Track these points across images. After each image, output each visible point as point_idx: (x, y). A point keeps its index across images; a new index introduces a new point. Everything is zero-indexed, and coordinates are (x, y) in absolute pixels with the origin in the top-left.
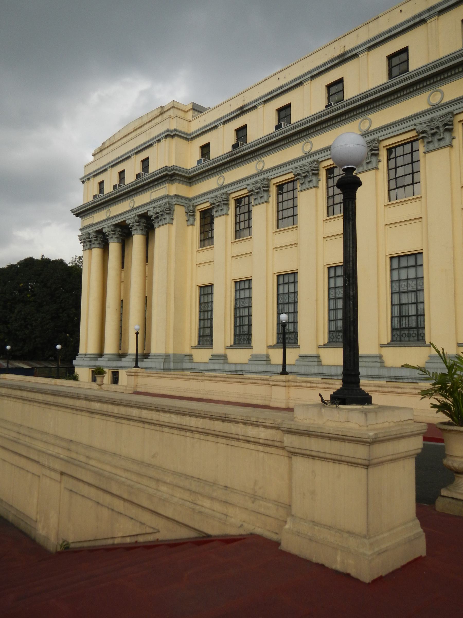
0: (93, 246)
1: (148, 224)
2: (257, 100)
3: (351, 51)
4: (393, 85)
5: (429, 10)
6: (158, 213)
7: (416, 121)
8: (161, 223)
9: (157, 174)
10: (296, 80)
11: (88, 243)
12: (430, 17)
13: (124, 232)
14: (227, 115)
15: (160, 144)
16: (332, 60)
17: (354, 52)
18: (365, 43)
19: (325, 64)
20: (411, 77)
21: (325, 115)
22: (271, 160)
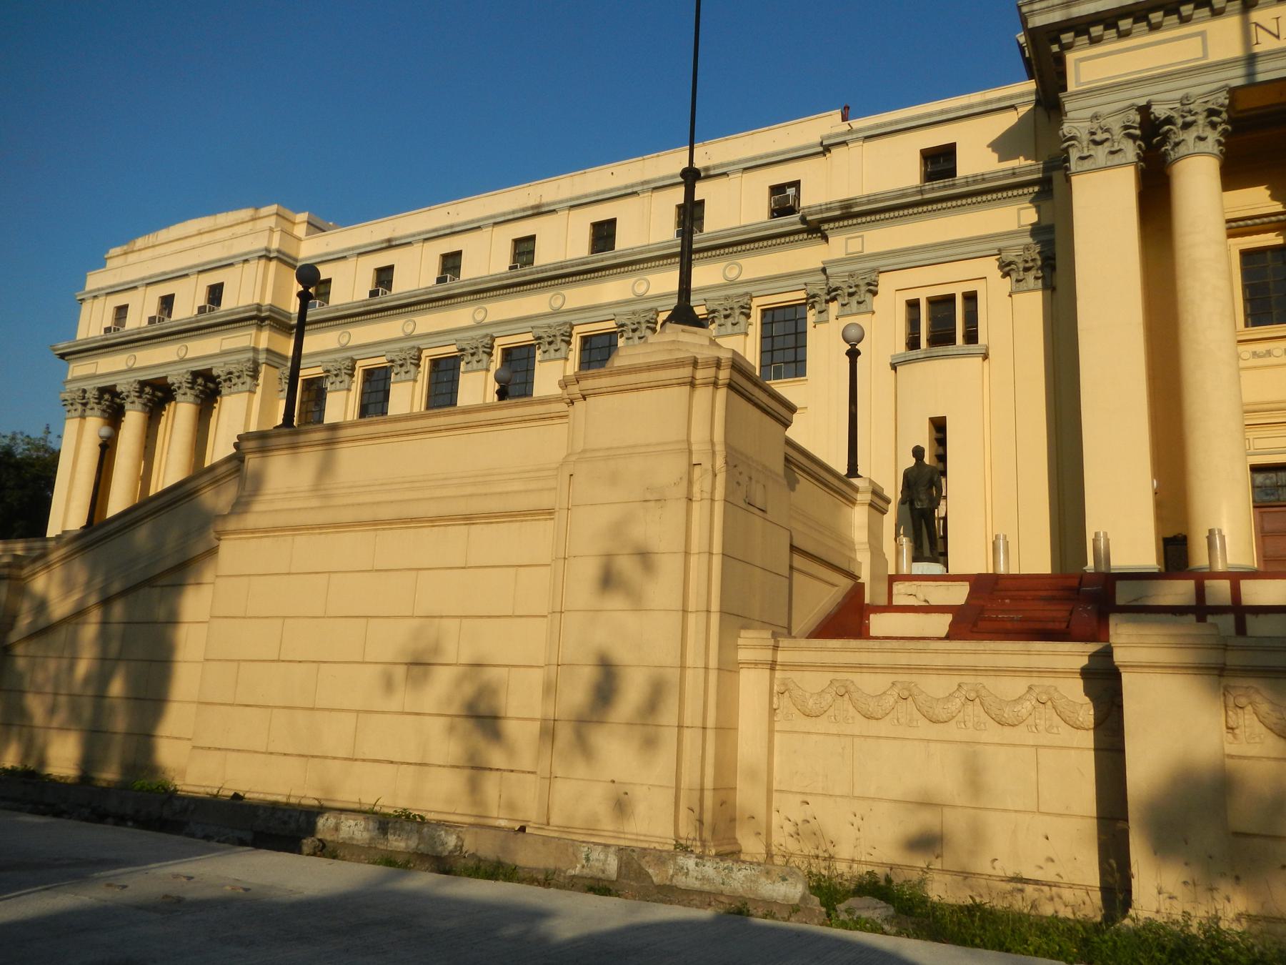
0: (88, 412)
1: (208, 389)
2: (414, 235)
3: (548, 205)
4: (593, 262)
5: (643, 183)
6: (231, 373)
7: (616, 310)
8: (234, 389)
9: (239, 313)
10: (472, 221)
11: (80, 407)
12: (643, 192)
13: (158, 395)
14: (365, 246)
15: (246, 265)
16: (524, 210)
17: (552, 208)
18: (567, 200)
19: (513, 212)
20: (615, 257)
21: (507, 278)
22: (427, 322)
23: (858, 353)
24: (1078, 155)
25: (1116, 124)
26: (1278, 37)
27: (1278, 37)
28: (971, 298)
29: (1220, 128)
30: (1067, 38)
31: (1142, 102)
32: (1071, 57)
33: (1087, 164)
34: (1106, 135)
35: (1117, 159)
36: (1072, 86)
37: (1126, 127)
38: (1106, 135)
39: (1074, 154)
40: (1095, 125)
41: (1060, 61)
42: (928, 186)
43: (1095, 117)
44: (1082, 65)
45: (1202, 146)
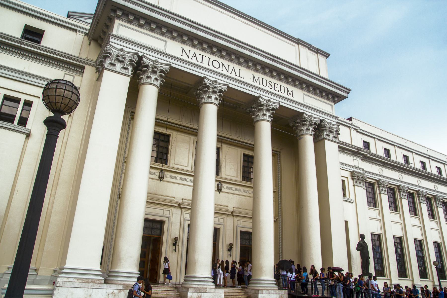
23: (63, 125)
24: (109, 62)
25: (128, 57)
26: (188, 57)
27: (188, 57)
28: (28, 104)
29: (162, 79)
30: (119, 13)
31: (140, 54)
32: (117, 22)
33: (112, 68)
34: (123, 60)
35: (124, 72)
36: (114, 32)
37: (131, 60)
38: (123, 60)
39: (108, 61)
40: (121, 53)
41: (111, 21)
42: (25, 42)
43: (121, 50)
44: (121, 27)
45: (156, 83)
